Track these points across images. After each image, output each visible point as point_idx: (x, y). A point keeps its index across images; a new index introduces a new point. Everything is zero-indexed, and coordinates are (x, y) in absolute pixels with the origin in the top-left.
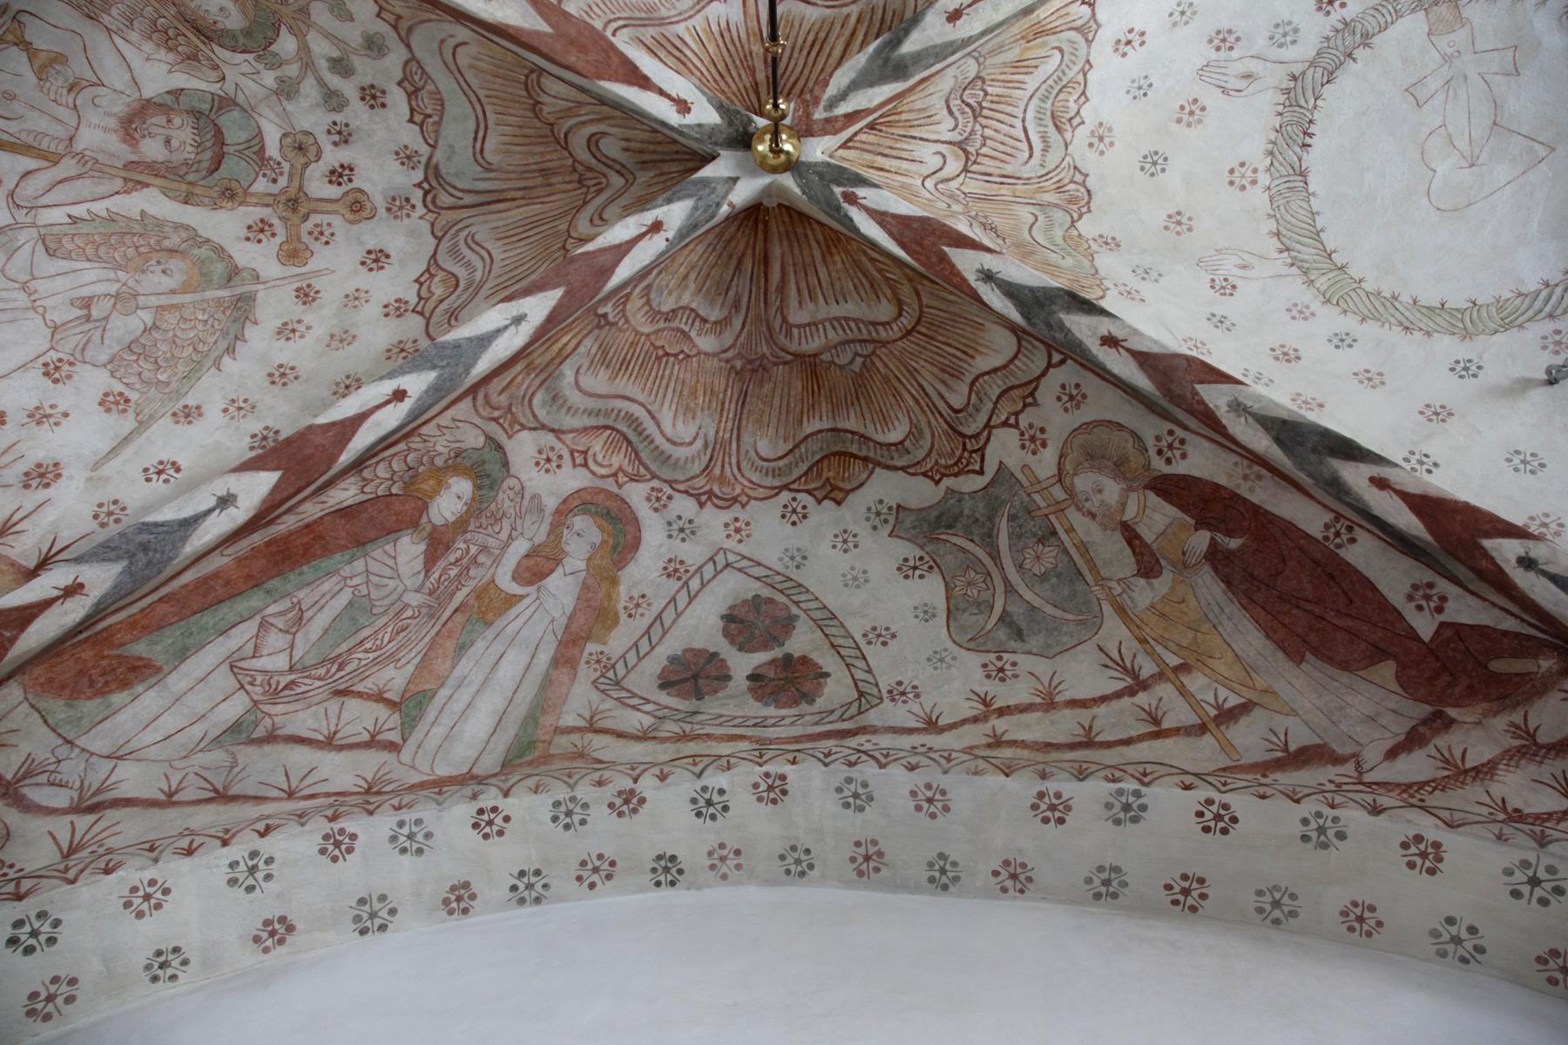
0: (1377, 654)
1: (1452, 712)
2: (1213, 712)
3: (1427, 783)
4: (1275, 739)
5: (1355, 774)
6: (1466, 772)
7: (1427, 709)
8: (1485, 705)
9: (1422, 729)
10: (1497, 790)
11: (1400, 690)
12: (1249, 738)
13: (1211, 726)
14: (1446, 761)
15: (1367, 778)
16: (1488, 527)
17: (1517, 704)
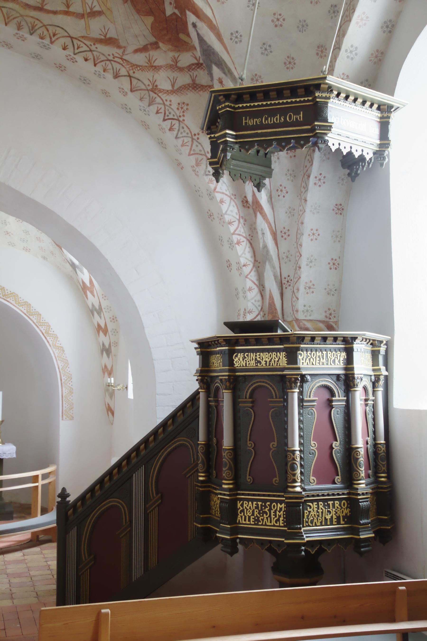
0: (150, 13)
1: (161, 44)
2: (89, 10)
3: (139, 66)
4: (103, 31)
5: (121, 54)
6: (152, 66)
7: (153, 40)
8: (170, 46)
9: (149, 46)
10: (156, 76)
11: (150, 29)
12: (96, 26)
13: (86, 16)
14: (149, 61)
15: (124, 57)
16: (190, 8)
17: (179, 51)
